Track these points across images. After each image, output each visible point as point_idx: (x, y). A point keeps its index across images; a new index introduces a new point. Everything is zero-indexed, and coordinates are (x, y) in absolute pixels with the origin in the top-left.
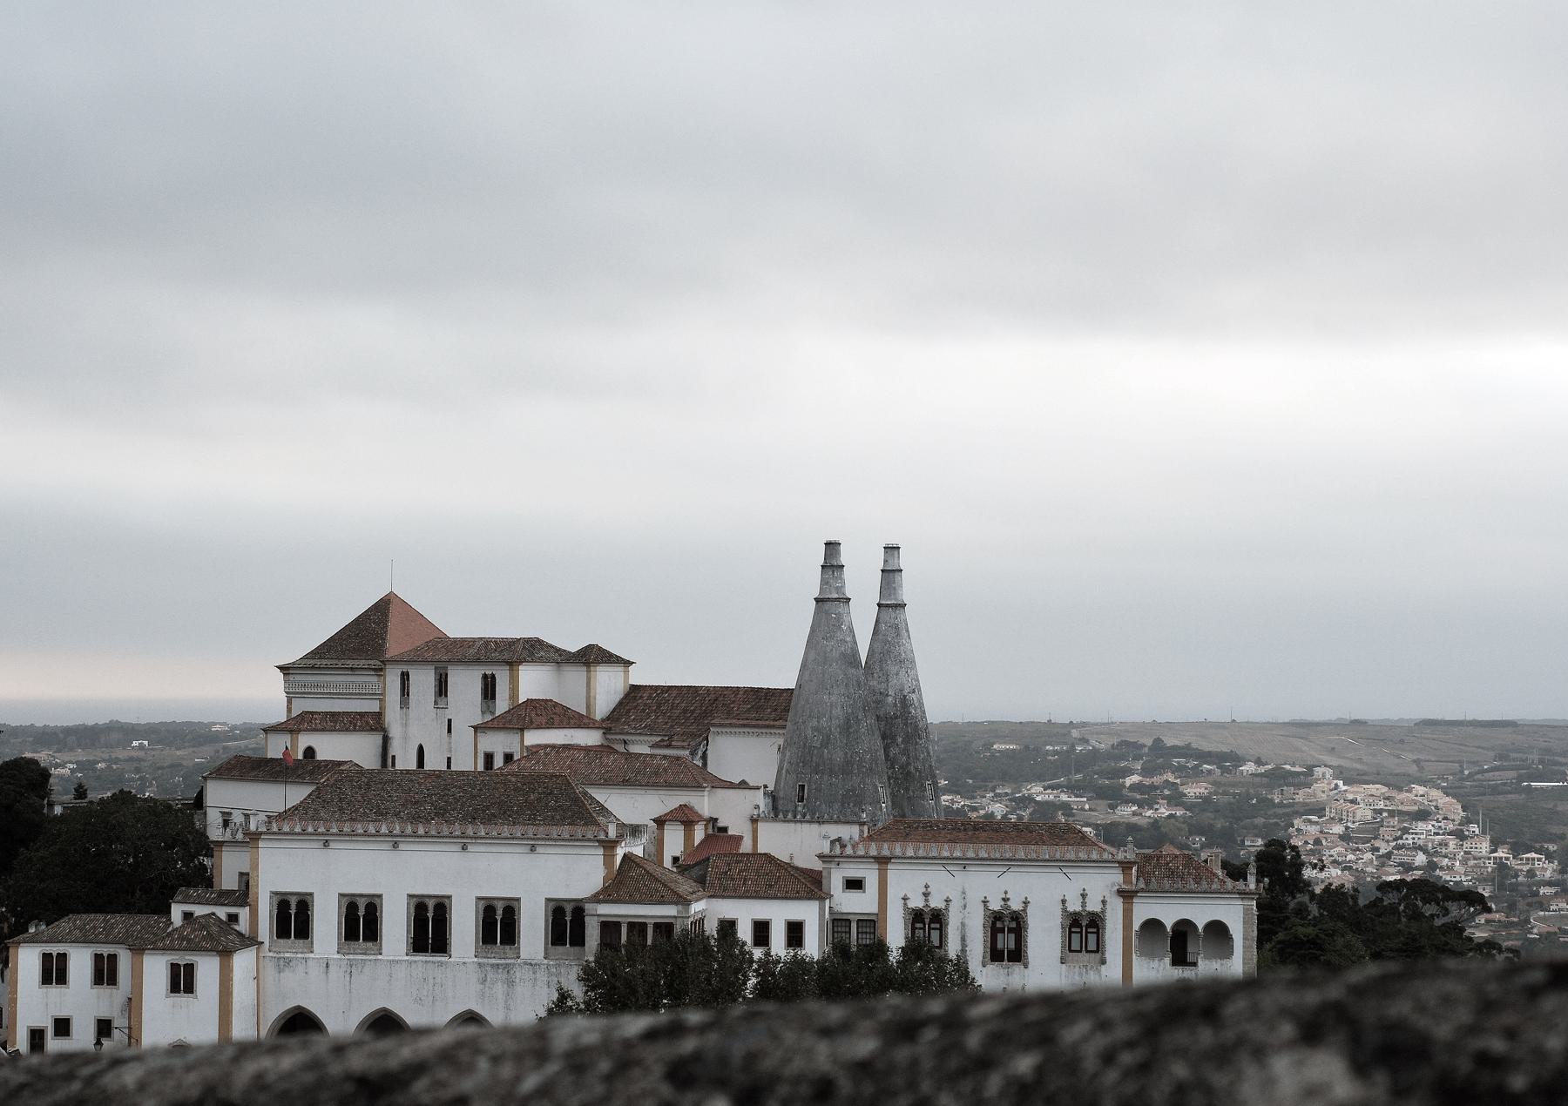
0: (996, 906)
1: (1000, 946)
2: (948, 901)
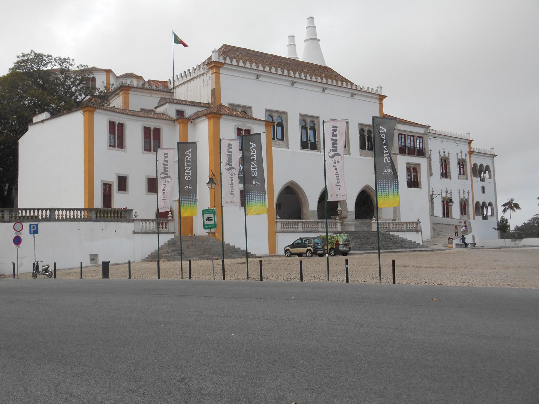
0: (442, 154)
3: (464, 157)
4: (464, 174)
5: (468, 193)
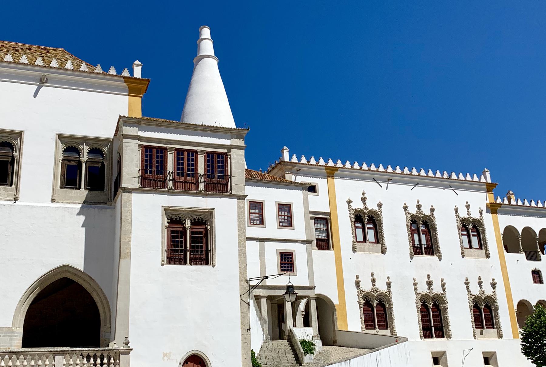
0: (413, 210)
1: (417, 242)
2: (380, 205)
3: (475, 215)
4: (481, 247)
5: (494, 285)
